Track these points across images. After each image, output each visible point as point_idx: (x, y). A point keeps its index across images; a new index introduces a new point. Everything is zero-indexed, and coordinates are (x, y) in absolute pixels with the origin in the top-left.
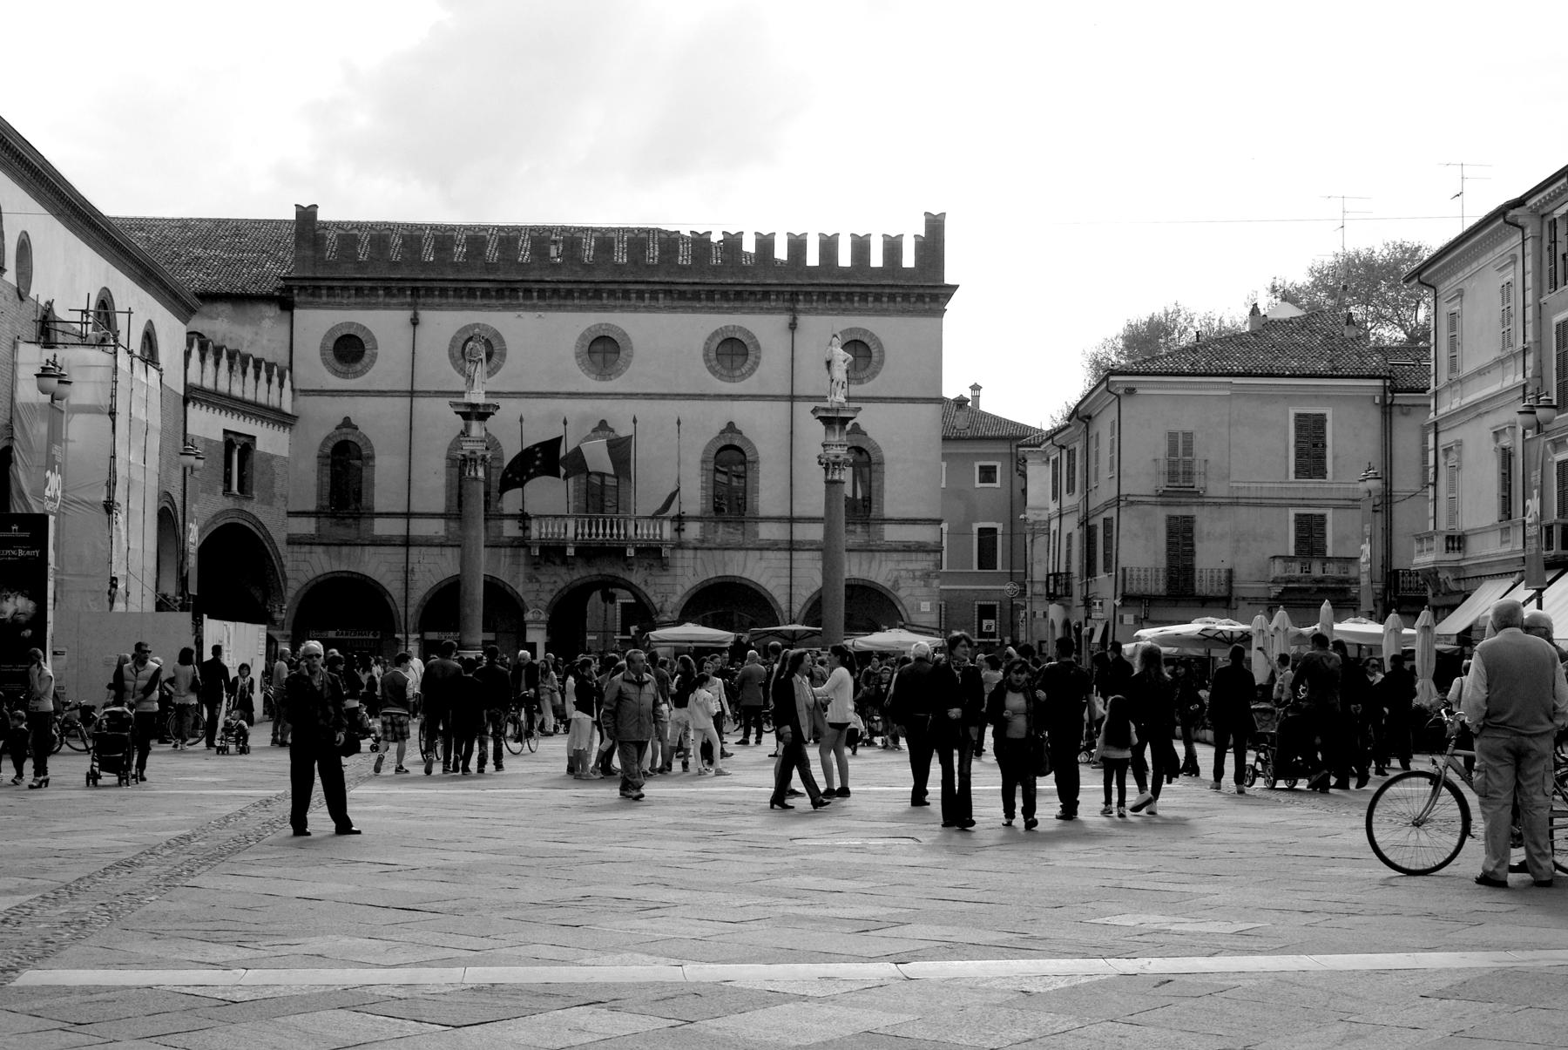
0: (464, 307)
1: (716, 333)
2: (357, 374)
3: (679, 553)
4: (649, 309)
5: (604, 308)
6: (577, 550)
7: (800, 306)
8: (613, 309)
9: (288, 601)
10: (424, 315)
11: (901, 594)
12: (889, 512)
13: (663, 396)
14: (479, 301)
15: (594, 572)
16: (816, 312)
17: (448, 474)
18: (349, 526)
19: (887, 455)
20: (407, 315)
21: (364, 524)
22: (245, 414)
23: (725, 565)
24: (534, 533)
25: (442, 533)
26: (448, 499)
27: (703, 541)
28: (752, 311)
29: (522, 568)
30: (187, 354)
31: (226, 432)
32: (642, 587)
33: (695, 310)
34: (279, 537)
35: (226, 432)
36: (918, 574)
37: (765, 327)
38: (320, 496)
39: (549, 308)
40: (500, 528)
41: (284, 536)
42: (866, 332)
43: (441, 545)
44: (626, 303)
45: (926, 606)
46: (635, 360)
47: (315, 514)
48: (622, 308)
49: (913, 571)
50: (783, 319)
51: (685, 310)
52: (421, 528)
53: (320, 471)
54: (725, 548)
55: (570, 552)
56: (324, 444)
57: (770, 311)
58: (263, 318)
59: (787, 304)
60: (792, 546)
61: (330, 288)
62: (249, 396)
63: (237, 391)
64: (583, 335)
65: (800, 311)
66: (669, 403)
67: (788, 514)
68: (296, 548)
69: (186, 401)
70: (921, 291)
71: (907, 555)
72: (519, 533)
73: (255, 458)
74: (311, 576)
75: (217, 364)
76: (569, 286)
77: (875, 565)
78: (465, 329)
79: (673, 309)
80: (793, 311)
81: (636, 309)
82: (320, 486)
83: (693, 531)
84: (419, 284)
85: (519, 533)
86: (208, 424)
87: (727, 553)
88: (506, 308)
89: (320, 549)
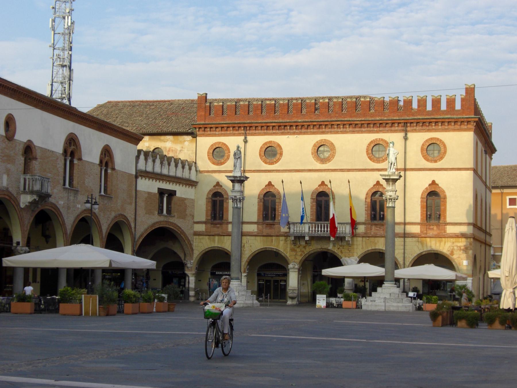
0: (265, 134)
1: (372, 142)
2: (222, 164)
3: (355, 239)
4: (342, 132)
5: (323, 133)
6: (310, 237)
7: (408, 129)
8: (327, 133)
9: (194, 259)
10: (249, 138)
11: (455, 257)
12: (448, 220)
13: (349, 170)
14: (271, 131)
15: (320, 247)
16: (415, 131)
17: (258, 205)
18: (218, 228)
19: (448, 194)
20: (243, 138)
21: (224, 226)
22: (170, 181)
23: (376, 244)
24: (292, 231)
25: (256, 230)
26: (258, 216)
27: (365, 233)
28: (388, 132)
29: (289, 246)
30: (138, 157)
31: (159, 189)
32: (340, 254)
33: (362, 132)
34: (188, 232)
35: (159, 189)
36: (462, 248)
37: (394, 138)
38: (207, 215)
39: (300, 133)
40: (279, 228)
41: (192, 231)
42: (438, 139)
44: (333, 130)
45: (465, 263)
46: (337, 155)
47: (205, 223)
48: (331, 133)
49: (460, 247)
50: (402, 134)
51: (358, 132)
52: (247, 228)
53: (207, 205)
54: (375, 237)
55: (307, 238)
56: (208, 193)
57: (395, 131)
58: (185, 141)
59: (403, 128)
60: (405, 235)
61: (211, 128)
62: (172, 174)
63: (165, 171)
64: (315, 145)
65: (409, 131)
66: (346, 174)
67: (403, 221)
68: (197, 237)
69: (136, 177)
70: (463, 120)
71: (457, 239)
72: (287, 230)
73: (174, 199)
74: (203, 248)
75: (154, 161)
76: (308, 124)
77: (442, 243)
78: (266, 143)
79: (353, 132)
80: (406, 132)
81: (337, 133)
83: (361, 229)
84: (246, 125)
85: (287, 230)
86: (148, 186)
87: (376, 239)
88: (283, 134)
89: (207, 237)
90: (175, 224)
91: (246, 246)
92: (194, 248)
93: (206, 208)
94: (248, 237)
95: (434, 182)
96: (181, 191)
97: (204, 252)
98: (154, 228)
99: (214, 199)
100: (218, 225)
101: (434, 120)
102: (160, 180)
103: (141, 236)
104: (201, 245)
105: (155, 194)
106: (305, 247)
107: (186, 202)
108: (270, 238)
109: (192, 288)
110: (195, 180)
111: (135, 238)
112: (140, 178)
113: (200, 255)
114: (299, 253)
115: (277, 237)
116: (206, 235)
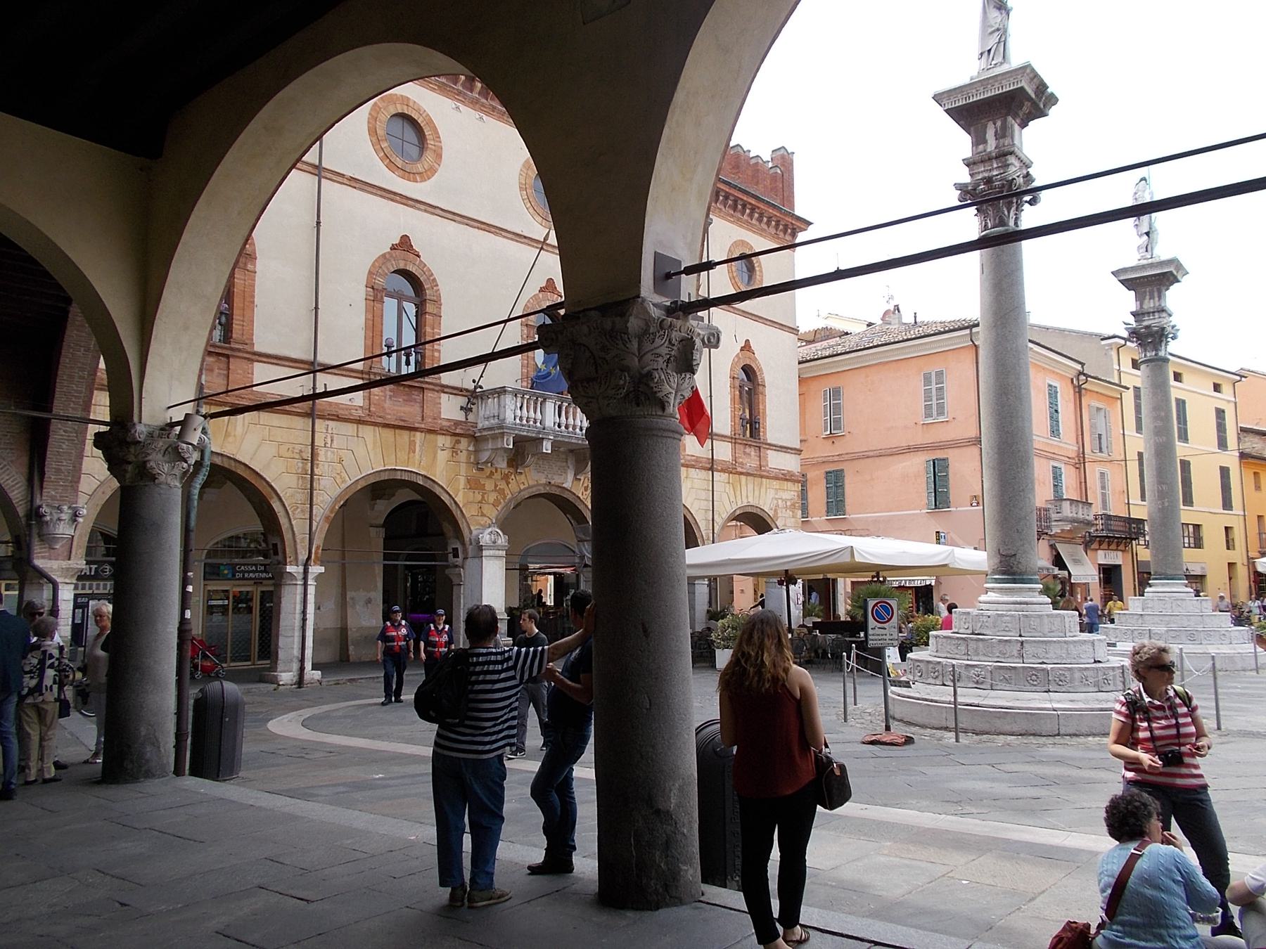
6: (555, 445)
15: (543, 481)
43: (360, 422)
49: (785, 501)
55: (547, 447)
72: (460, 416)
77: (763, 490)
85: (460, 416)
94: (330, 423)
95: (747, 347)
101: (753, 201)
106: (506, 478)
108: (406, 434)
114: (492, 497)
115: (428, 436)
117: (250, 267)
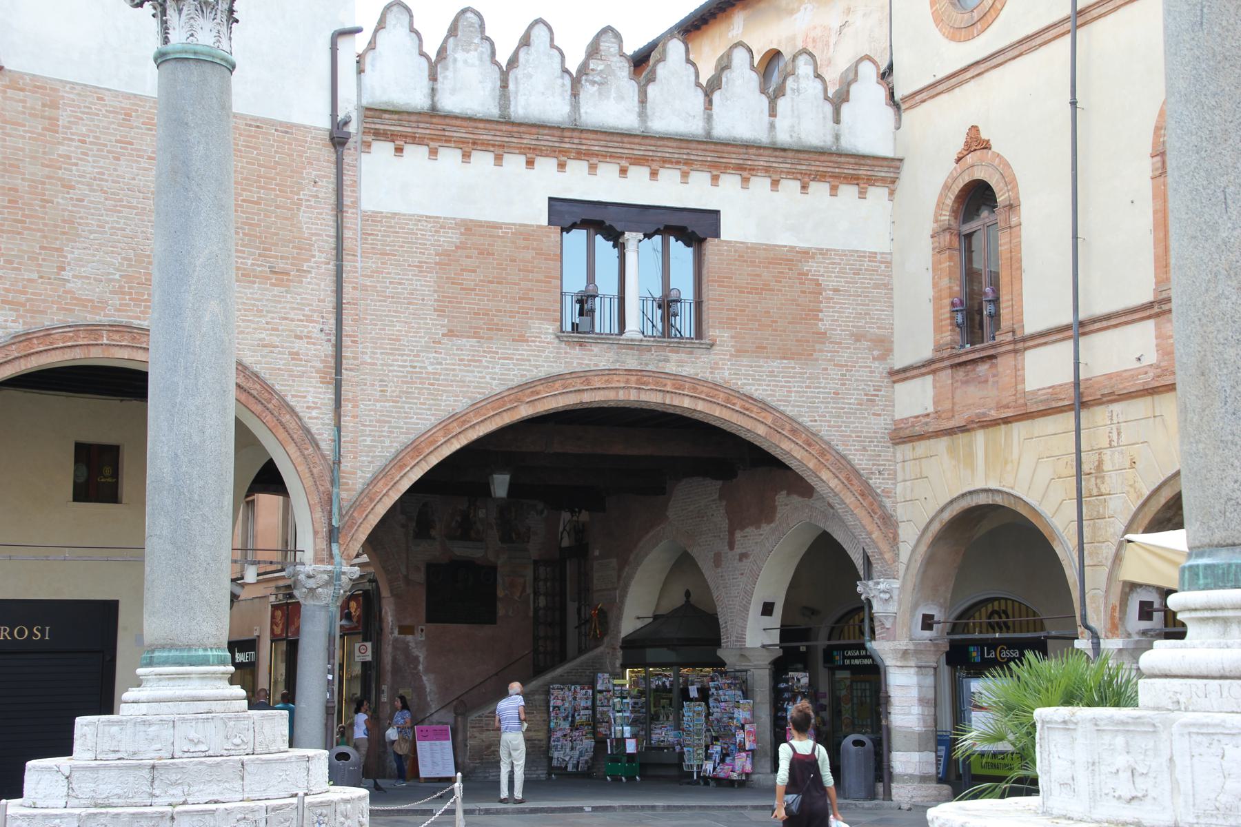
2: (984, 20)
25: (1151, 357)
38: (938, 329)
41: (880, 425)
47: (926, 367)
56: (940, 205)
68: (905, 451)
82: (937, 300)
90: (716, 386)
91: (1107, 466)
92: (901, 512)
93: (935, 285)
94: (1116, 407)
96: (751, 213)
97: (936, 527)
98: (525, 412)
99: (966, 229)
100: (983, 368)
102: (562, 156)
103: (415, 449)
104: (926, 490)
105: (525, 233)
107: (811, 266)
109: (907, 734)
110: (884, 149)
111: (338, 462)
112: (382, 150)
113: (923, 548)
116: (938, 434)
117: (1014, 220)
